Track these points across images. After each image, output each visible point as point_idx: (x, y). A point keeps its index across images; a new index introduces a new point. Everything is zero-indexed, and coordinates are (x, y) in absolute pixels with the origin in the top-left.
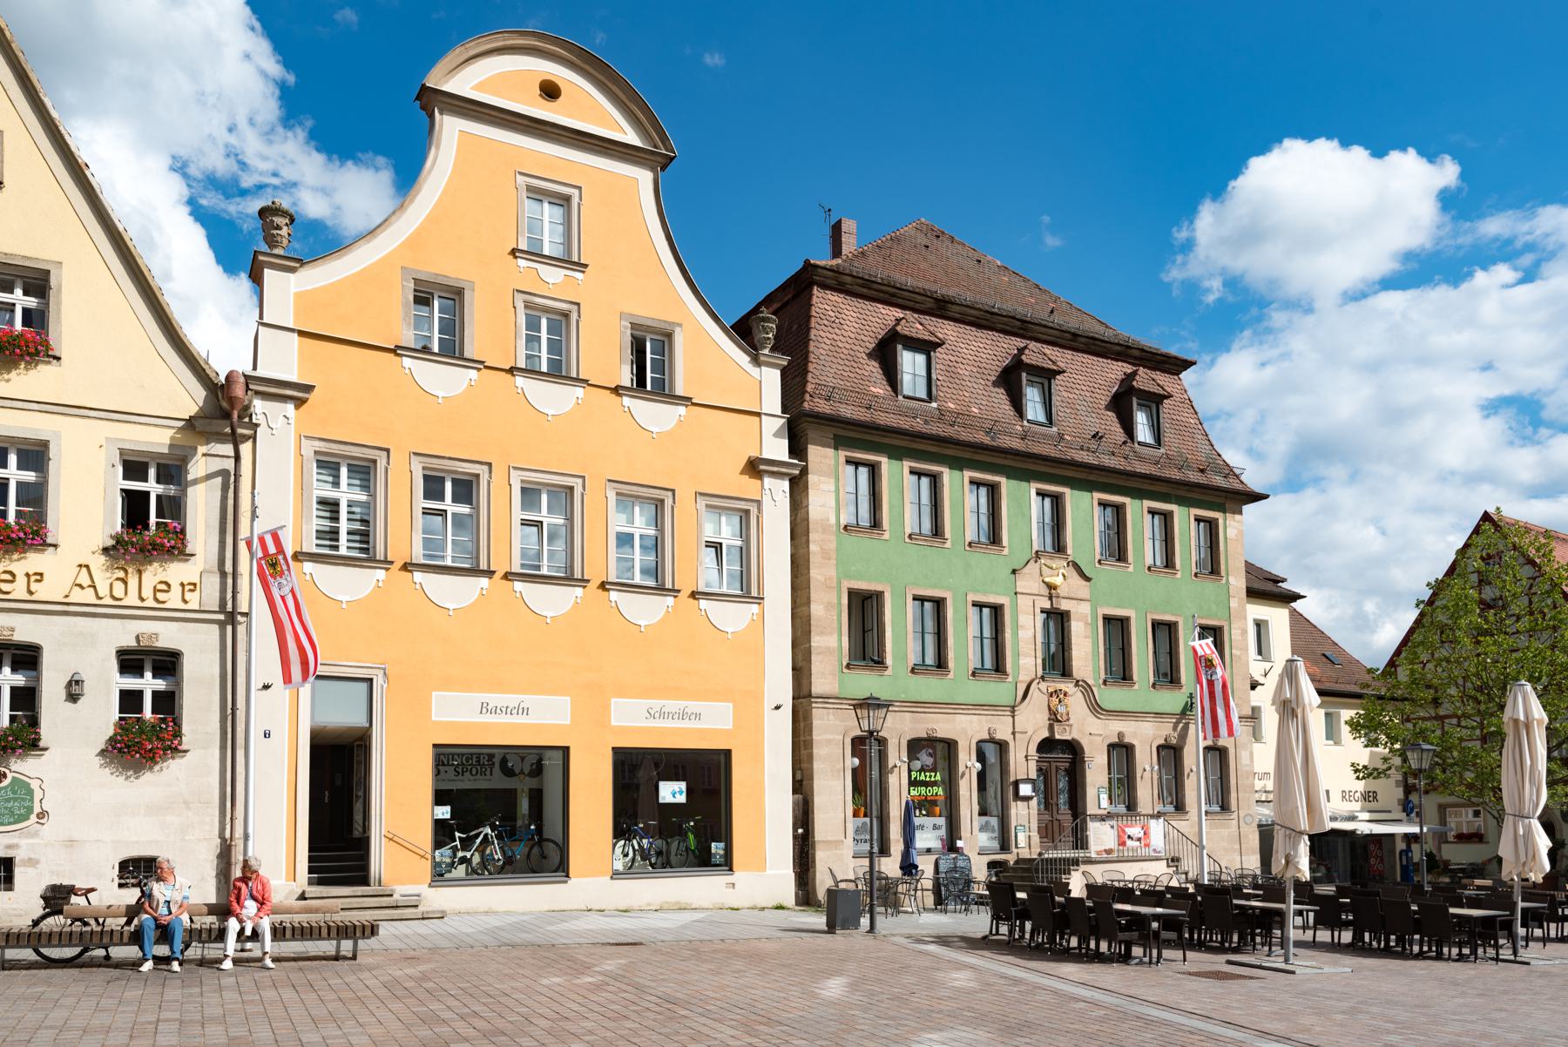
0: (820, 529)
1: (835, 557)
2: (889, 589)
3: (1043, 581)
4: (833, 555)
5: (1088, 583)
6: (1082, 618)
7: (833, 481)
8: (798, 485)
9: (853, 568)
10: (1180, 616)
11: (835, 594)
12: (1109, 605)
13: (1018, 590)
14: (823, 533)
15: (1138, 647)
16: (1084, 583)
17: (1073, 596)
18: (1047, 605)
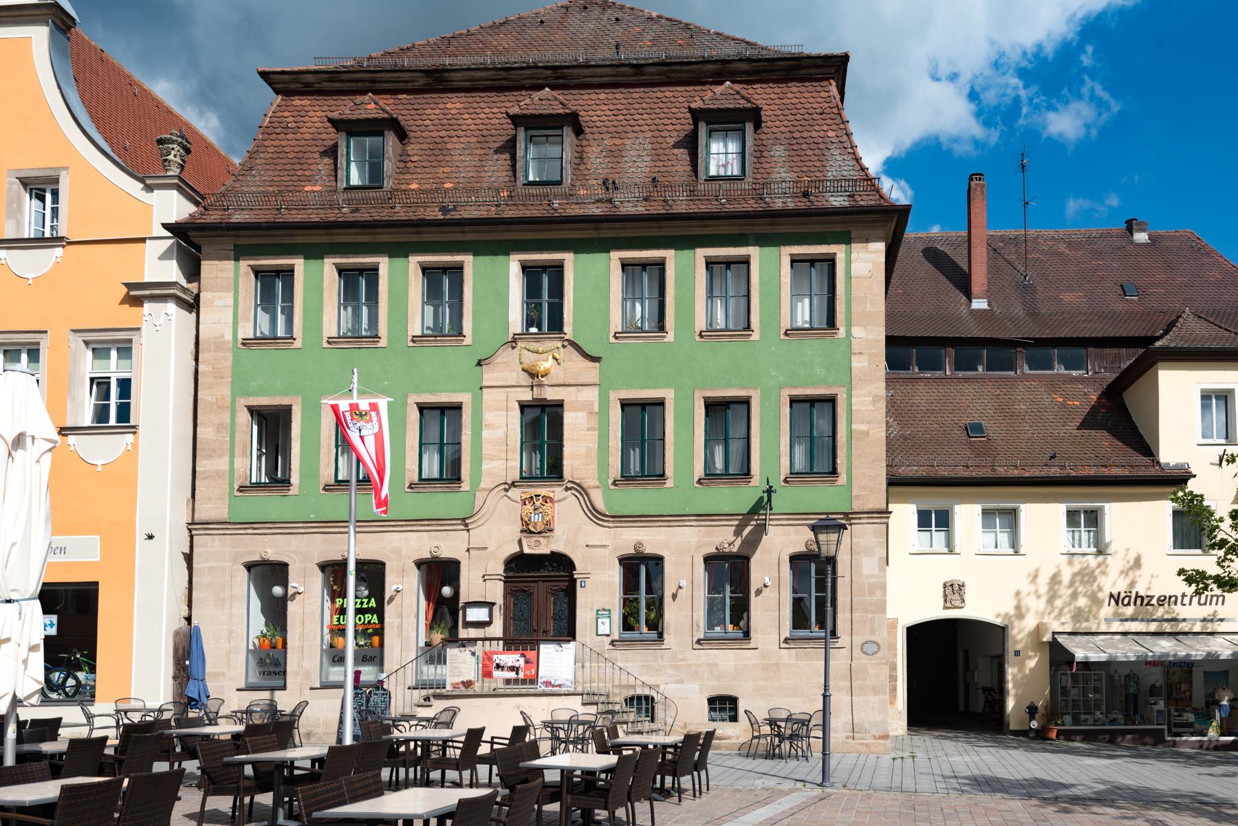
0: (213, 348)
1: (230, 375)
2: (299, 402)
3: (523, 370)
4: (228, 373)
5: (597, 364)
6: (585, 406)
7: (231, 294)
8: (193, 305)
9: (254, 384)
10: (754, 388)
11: (228, 414)
12: (629, 386)
13: (485, 383)
14: (215, 351)
15: (676, 434)
16: (592, 364)
17: (572, 382)
18: (527, 396)
